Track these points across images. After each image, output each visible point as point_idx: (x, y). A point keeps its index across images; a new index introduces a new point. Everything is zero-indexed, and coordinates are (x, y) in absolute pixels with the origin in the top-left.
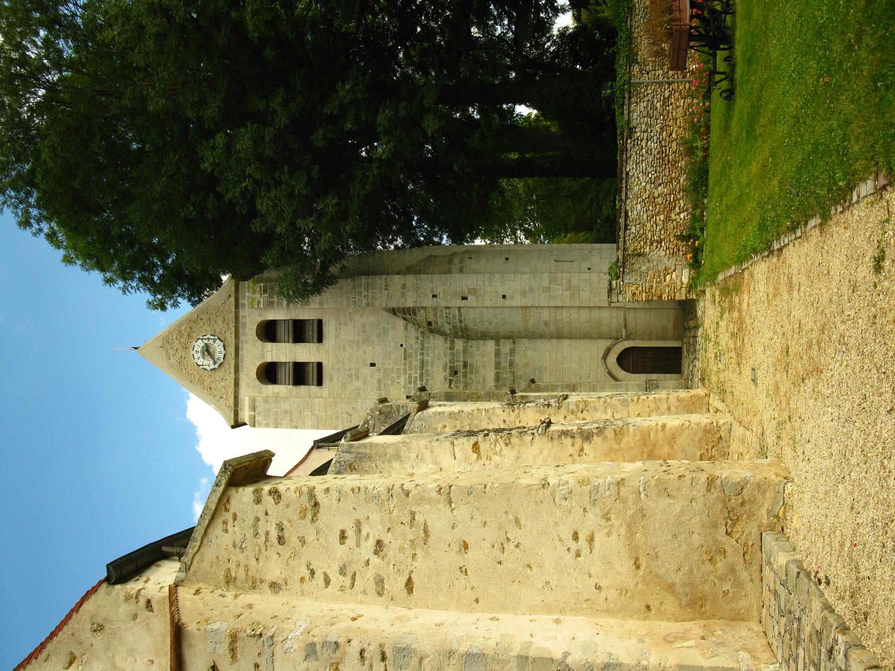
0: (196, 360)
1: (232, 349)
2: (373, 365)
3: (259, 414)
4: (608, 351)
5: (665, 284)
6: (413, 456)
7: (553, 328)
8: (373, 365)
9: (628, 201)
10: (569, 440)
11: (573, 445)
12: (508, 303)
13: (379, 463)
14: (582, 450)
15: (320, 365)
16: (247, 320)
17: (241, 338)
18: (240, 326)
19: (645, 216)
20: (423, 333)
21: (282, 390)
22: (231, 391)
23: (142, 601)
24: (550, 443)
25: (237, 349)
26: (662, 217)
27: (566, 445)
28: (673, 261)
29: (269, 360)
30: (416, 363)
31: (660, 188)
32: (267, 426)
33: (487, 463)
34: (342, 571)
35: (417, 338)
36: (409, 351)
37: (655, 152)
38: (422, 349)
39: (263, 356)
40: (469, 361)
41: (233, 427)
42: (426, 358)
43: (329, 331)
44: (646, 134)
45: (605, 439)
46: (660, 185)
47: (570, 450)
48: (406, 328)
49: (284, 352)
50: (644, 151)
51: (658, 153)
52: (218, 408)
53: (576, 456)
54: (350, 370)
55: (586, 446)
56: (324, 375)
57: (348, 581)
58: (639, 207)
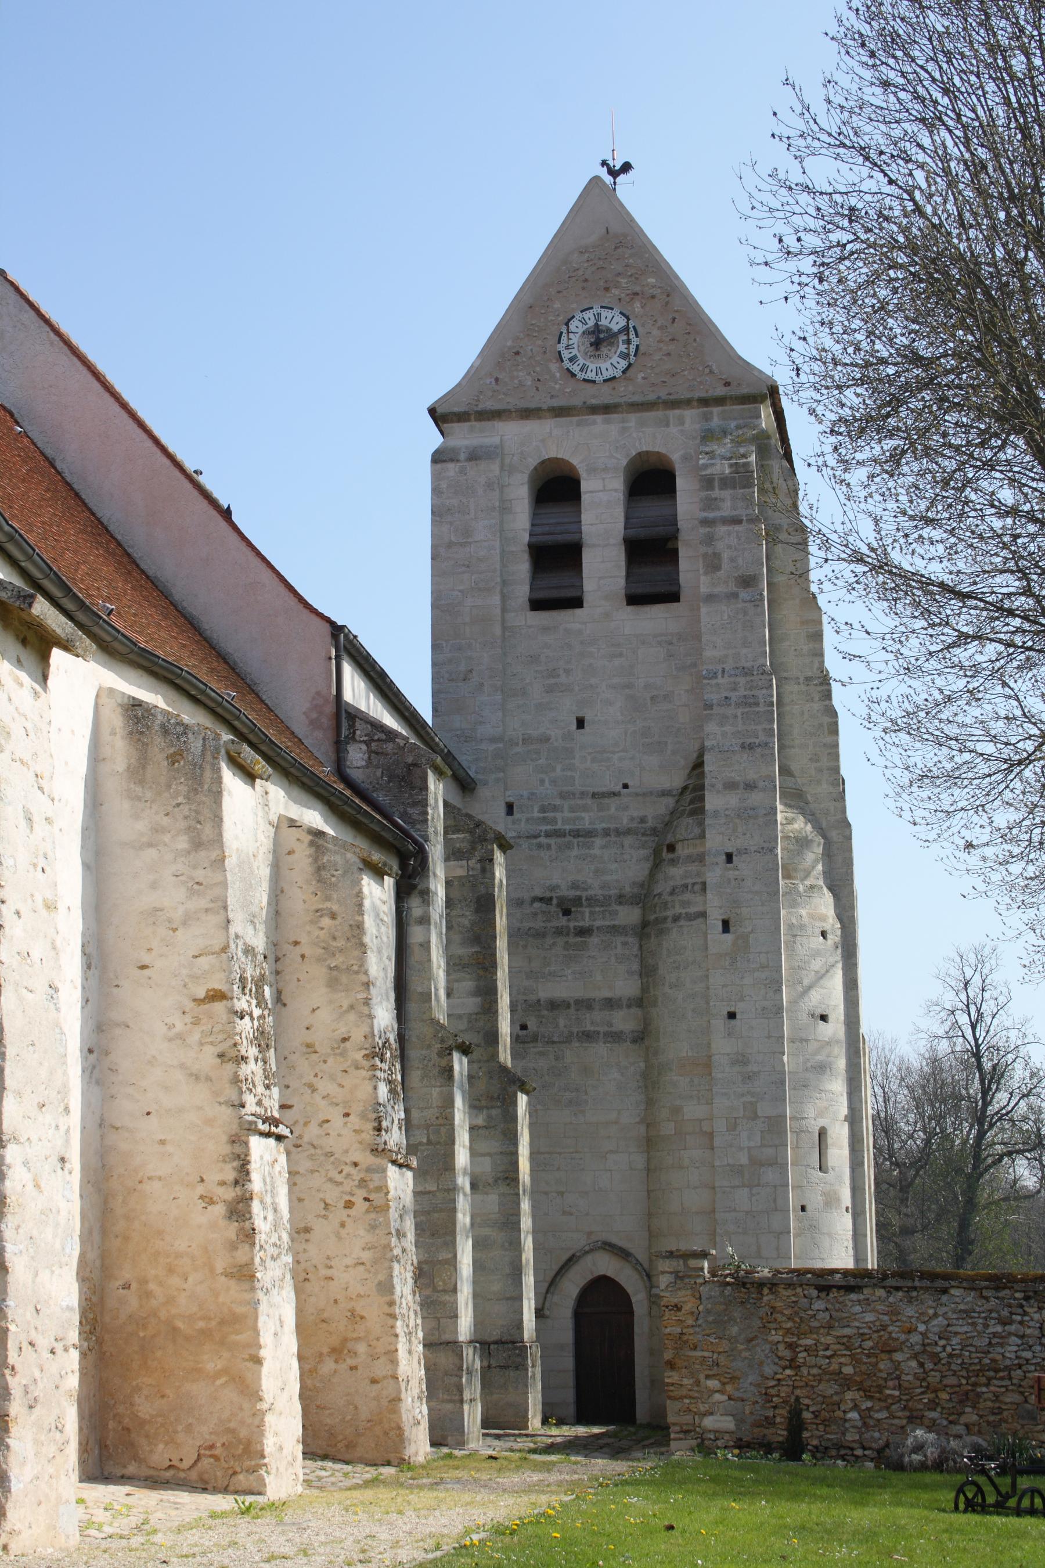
0: (579, 316)
1: (605, 396)
2: (581, 723)
3: (462, 471)
4: (623, 1254)
5: (702, 1377)
6: (199, 874)
7: (668, 1128)
8: (581, 723)
9: (881, 1293)
10: (230, 1175)
11: (222, 1183)
12: (719, 1023)
13: (185, 810)
14: (212, 1202)
15: (576, 602)
16: (673, 430)
17: (633, 419)
18: (660, 414)
19: (847, 1331)
20: (654, 831)
21: (521, 519)
22: (513, 402)
24: (224, 1138)
25: (607, 409)
26: (848, 1370)
27: (222, 1170)
29: (584, 486)
30: (586, 820)
31: (914, 1364)
32: (436, 491)
33: (188, 1019)
35: (643, 820)
36: (613, 804)
37: (996, 1353)
38: (618, 833)
39: (592, 470)
40: (594, 940)
41: (432, 411)
42: (598, 842)
43: (656, 618)
44: (1037, 1333)
45: (233, 1247)
46: (921, 1365)
47: (213, 1176)
48: (665, 793)
49: (603, 516)
50: (999, 1329)
51: (993, 1360)
52: (473, 376)
53: (200, 1190)
54: (567, 672)
55: (219, 1210)
56: (554, 614)
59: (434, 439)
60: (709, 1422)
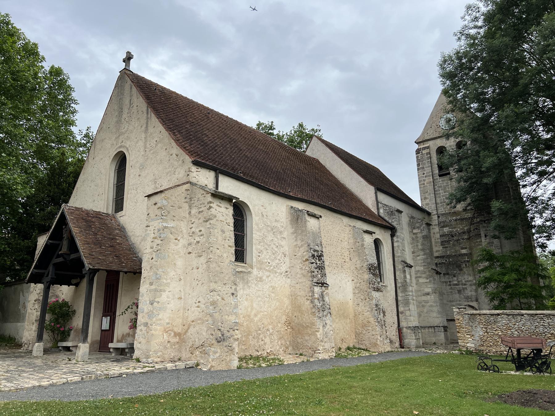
22: (432, 137)
23: (188, 173)
28: (477, 338)
34: (193, 233)
57: (191, 235)
58: (504, 322)
59: (416, 147)
60: (468, 345)
